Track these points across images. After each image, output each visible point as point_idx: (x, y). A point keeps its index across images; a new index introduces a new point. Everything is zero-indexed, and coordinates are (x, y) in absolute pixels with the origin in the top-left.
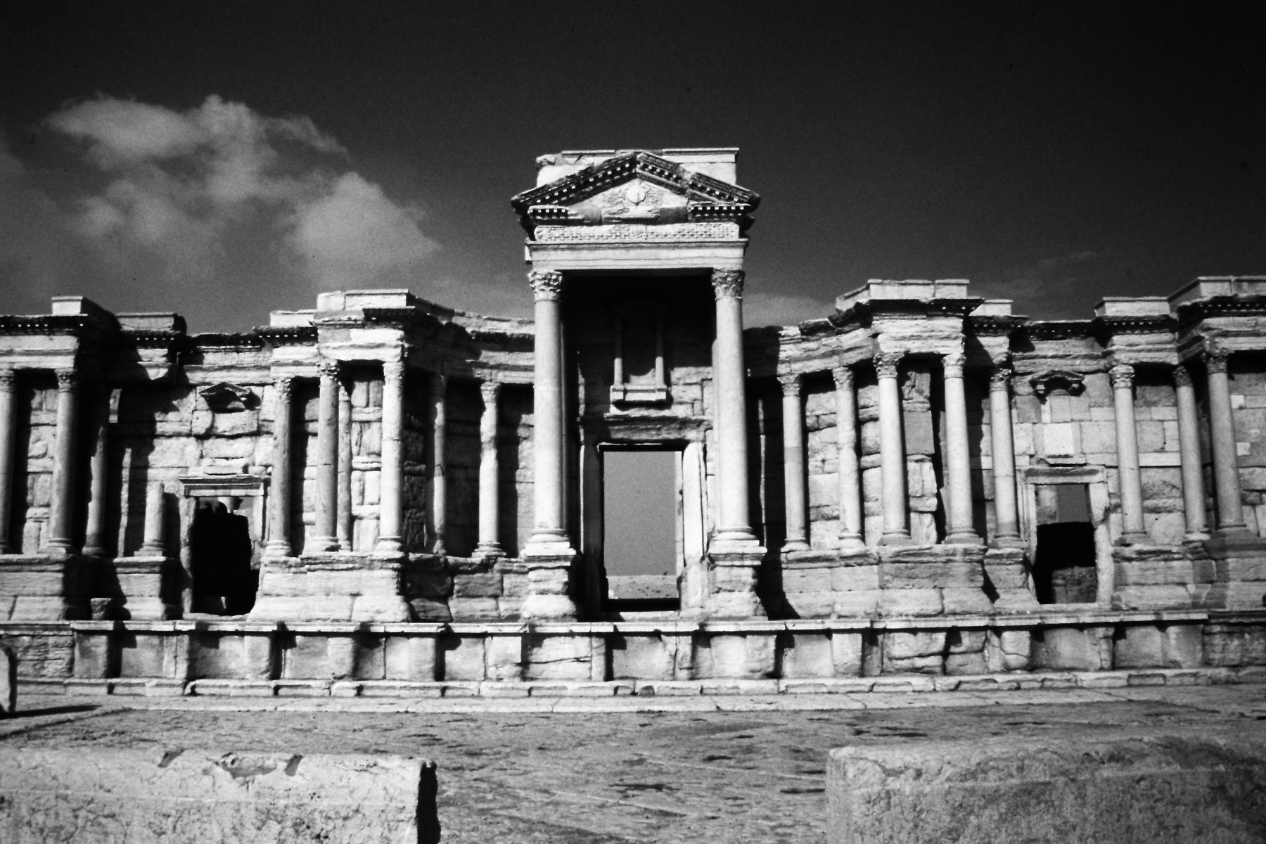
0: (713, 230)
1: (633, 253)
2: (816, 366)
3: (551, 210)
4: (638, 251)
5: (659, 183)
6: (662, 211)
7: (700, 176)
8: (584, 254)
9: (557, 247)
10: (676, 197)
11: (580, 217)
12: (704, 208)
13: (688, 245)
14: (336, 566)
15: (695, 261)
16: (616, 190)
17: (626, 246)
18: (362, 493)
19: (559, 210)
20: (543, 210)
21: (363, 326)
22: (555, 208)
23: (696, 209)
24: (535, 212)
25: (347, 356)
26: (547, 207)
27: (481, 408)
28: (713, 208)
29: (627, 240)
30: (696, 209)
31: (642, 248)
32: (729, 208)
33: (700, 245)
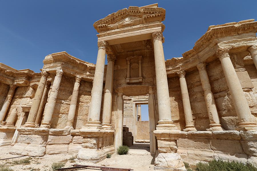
1: (126, 33)
2: (190, 66)
3: (103, 25)
12: (148, 17)
14: (26, 133)
22: (104, 25)
23: (145, 18)
25: (48, 70)
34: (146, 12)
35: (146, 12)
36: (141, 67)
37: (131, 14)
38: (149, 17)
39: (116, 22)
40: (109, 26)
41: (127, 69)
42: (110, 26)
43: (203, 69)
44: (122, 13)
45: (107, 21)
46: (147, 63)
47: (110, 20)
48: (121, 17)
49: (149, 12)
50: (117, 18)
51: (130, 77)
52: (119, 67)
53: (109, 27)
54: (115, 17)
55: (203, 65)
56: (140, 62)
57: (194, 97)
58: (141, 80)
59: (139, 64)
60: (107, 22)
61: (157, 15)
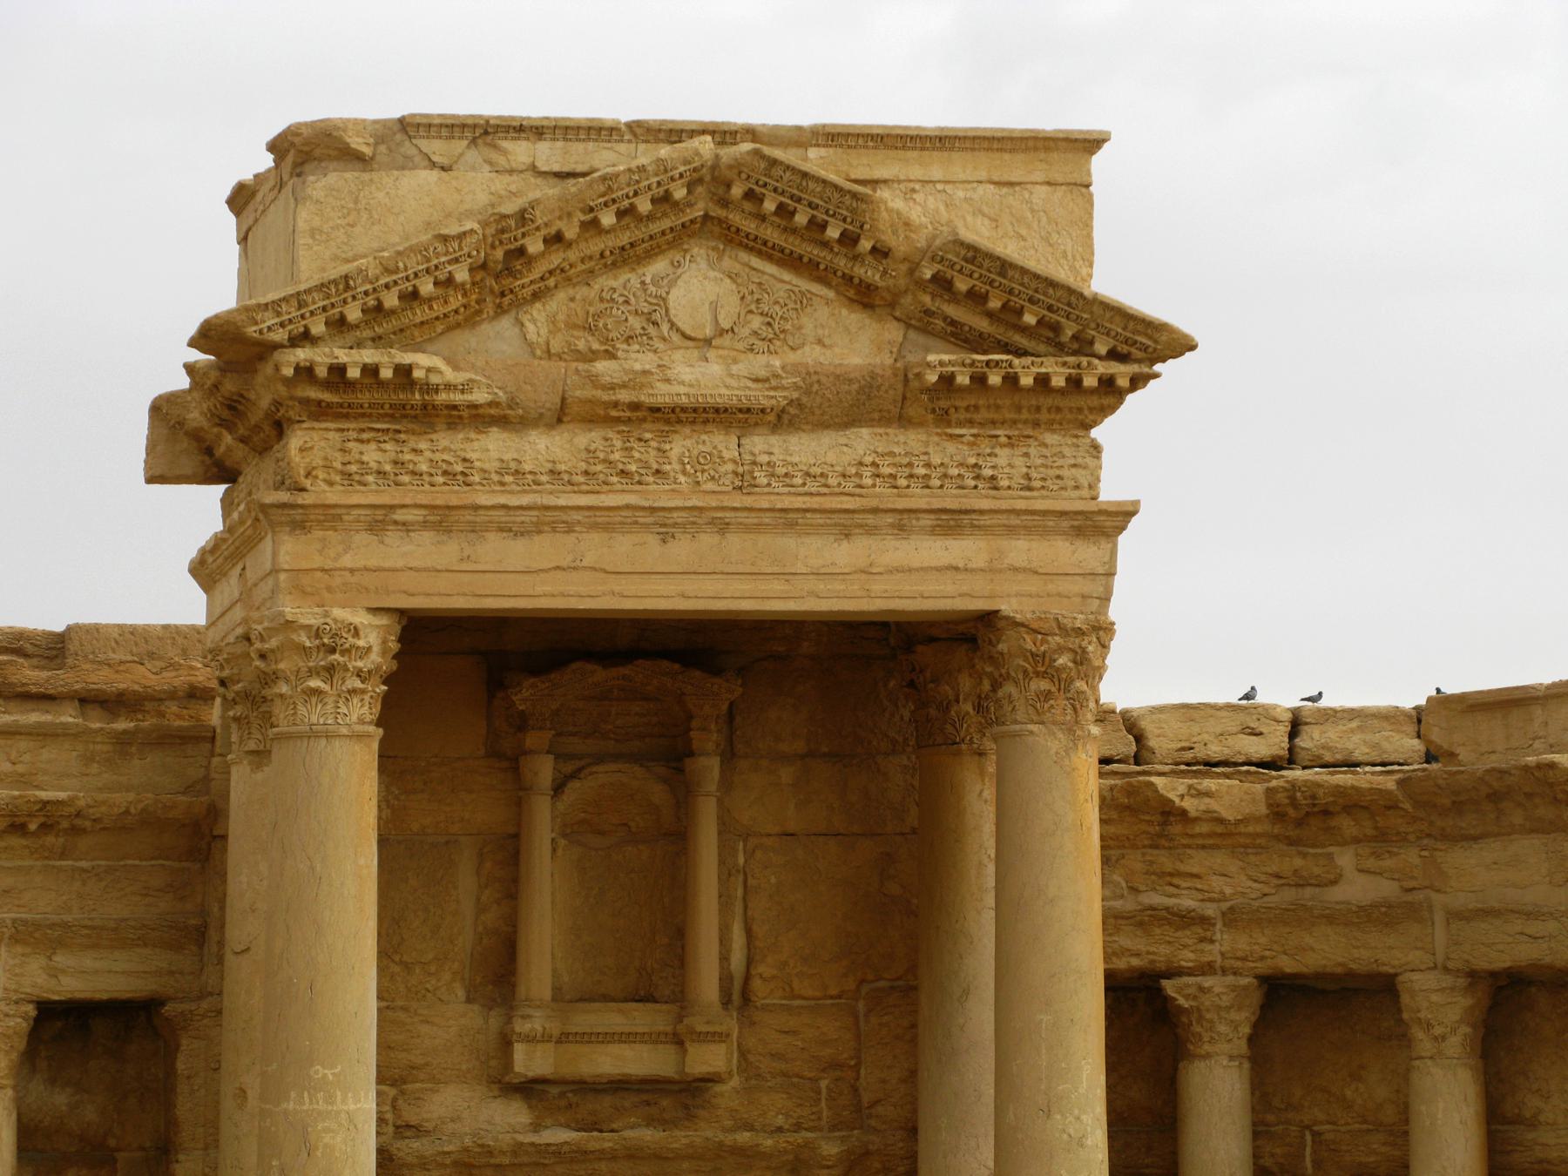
0: (1003, 457)
1: (682, 550)
2: (1323, 952)
3: (371, 371)
4: (708, 539)
5: (792, 262)
6: (811, 380)
7: (974, 255)
8: (496, 550)
9: (381, 521)
10: (853, 318)
11: (480, 396)
12: (979, 380)
13: (902, 522)
15: (932, 586)
16: (625, 280)
17: (664, 524)
19: (404, 371)
22: (386, 360)
23: (947, 380)
24: (305, 372)
28: (1011, 380)
29: (659, 495)
30: (947, 380)
31: (723, 528)
32: (1075, 383)
33: (951, 522)
34: (962, 285)
37: (750, 226)
38: (995, 379)
39: (527, 292)
40: (449, 387)
42: (465, 388)
43: (1454, 1045)
45: (426, 288)
46: (786, 774)
47: (462, 275)
49: (995, 304)
50: (556, 259)
51: (565, 998)
53: (443, 397)
54: (534, 246)
55: (1467, 1002)
56: (709, 768)
58: (708, 1059)
61: (1090, 381)
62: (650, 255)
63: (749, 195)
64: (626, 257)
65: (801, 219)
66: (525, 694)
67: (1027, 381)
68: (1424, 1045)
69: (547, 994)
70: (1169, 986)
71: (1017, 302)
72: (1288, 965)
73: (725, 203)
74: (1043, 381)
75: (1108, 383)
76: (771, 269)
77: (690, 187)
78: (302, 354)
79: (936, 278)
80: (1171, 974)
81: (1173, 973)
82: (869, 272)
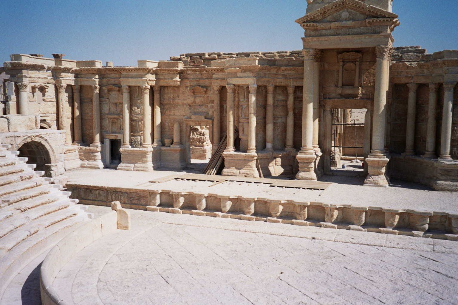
2: (422, 81)
18: (243, 131)
20: (307, 25)
21: (242, 72)
26: (309, 24)
27: (287, 95)
34: (371, 11)
35: (371, 11)
36: (359, 68)
41: (338, 71)
43: (434, 91)
44: (338, 5)
45: (316, 16)
46: (368, 63)
47: (319, 14)
48: (335, 9)
51: (343, 85)
52: (326, 66)
54: (326, 11)
57: (423, 117)
59: (356, 65)
60: (314, 17)
62: (340, 10)
63: (349, 3)
64: (337, 11)
65: (354, 5)
66: (339, 56)
67: (378, 21)
68: (431, 91)
69: (341, 85)
70: (407, 85)
71: (377, 12)
72: (419, 83)
73: (347, 4)
74: (380, 21)
75: (387, 20)
76: (352, 11)
77: (343, 3)
78: (304, 24)
79: (369, 10)
80: (408, 83)
81: (408, 83)
82: (362, 10)
